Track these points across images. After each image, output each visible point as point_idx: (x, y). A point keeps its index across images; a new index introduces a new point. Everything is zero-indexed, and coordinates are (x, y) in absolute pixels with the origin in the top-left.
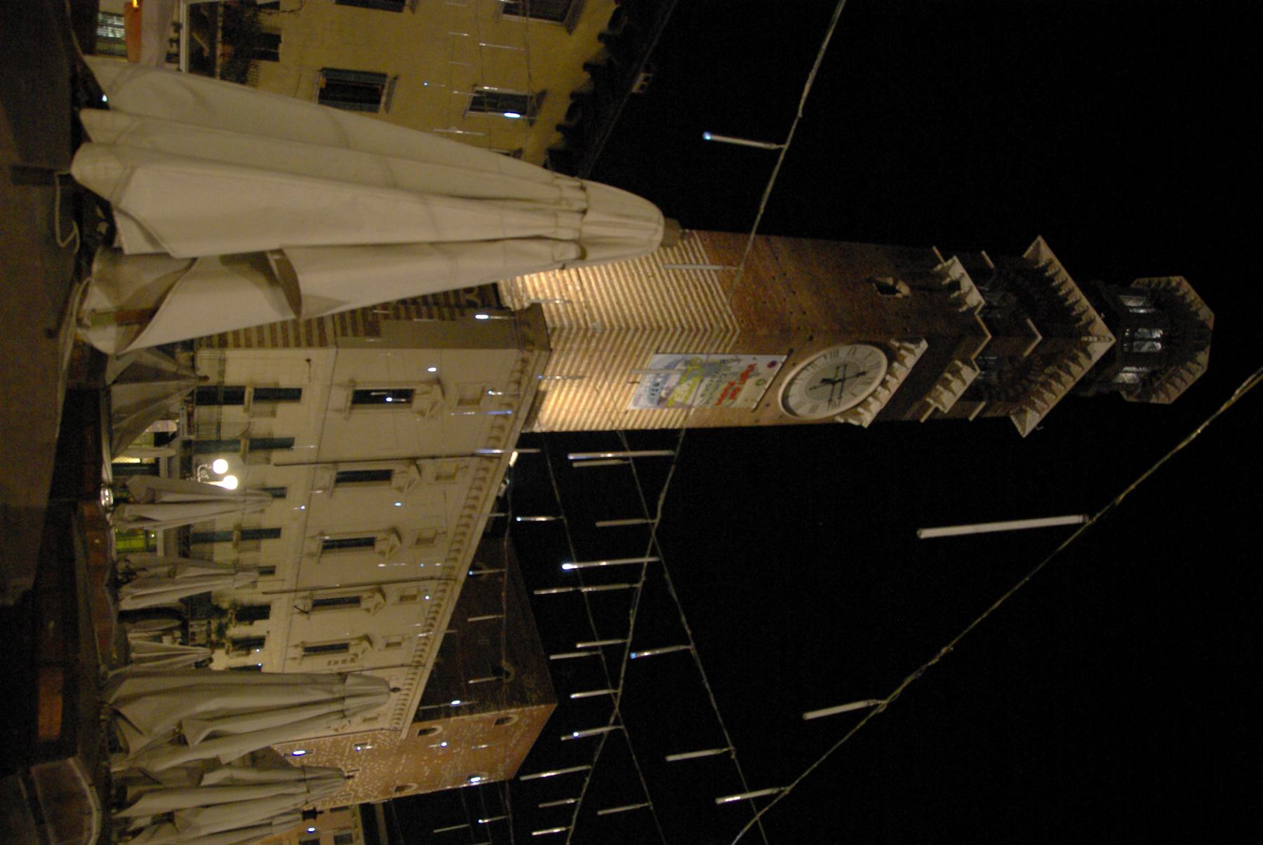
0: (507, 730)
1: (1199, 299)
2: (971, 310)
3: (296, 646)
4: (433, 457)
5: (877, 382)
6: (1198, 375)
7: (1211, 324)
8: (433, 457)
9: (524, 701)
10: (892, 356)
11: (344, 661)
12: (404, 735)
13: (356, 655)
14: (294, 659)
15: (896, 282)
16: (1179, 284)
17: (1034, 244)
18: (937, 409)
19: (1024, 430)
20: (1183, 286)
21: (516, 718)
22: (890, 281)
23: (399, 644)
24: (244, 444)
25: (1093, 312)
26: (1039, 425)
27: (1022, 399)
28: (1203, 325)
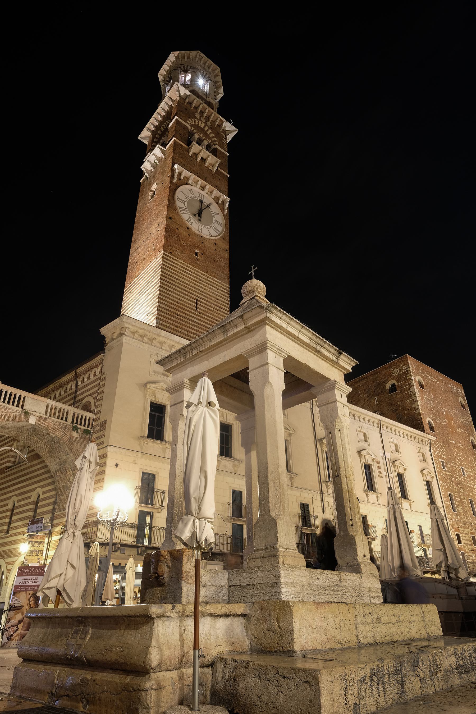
0: (427, 383)
1: (166, 62)
2: (163, 152)
6: (202, 55)
7: (177, 53)
9: (407, 373)
10: (186, 182)
11: (379, 468)
12: (434, 438)
13: (373, 459)
14: (377, 497)
15: (151, 191)
16: (162, 75)
17: (141, 140)
19: (234, 130)
20: (162, 73)
21: (418, 378)
22: (151, 193)
23: (365, 434)
25: (166, 99)
26: (230, 122)
28: (177, 58)
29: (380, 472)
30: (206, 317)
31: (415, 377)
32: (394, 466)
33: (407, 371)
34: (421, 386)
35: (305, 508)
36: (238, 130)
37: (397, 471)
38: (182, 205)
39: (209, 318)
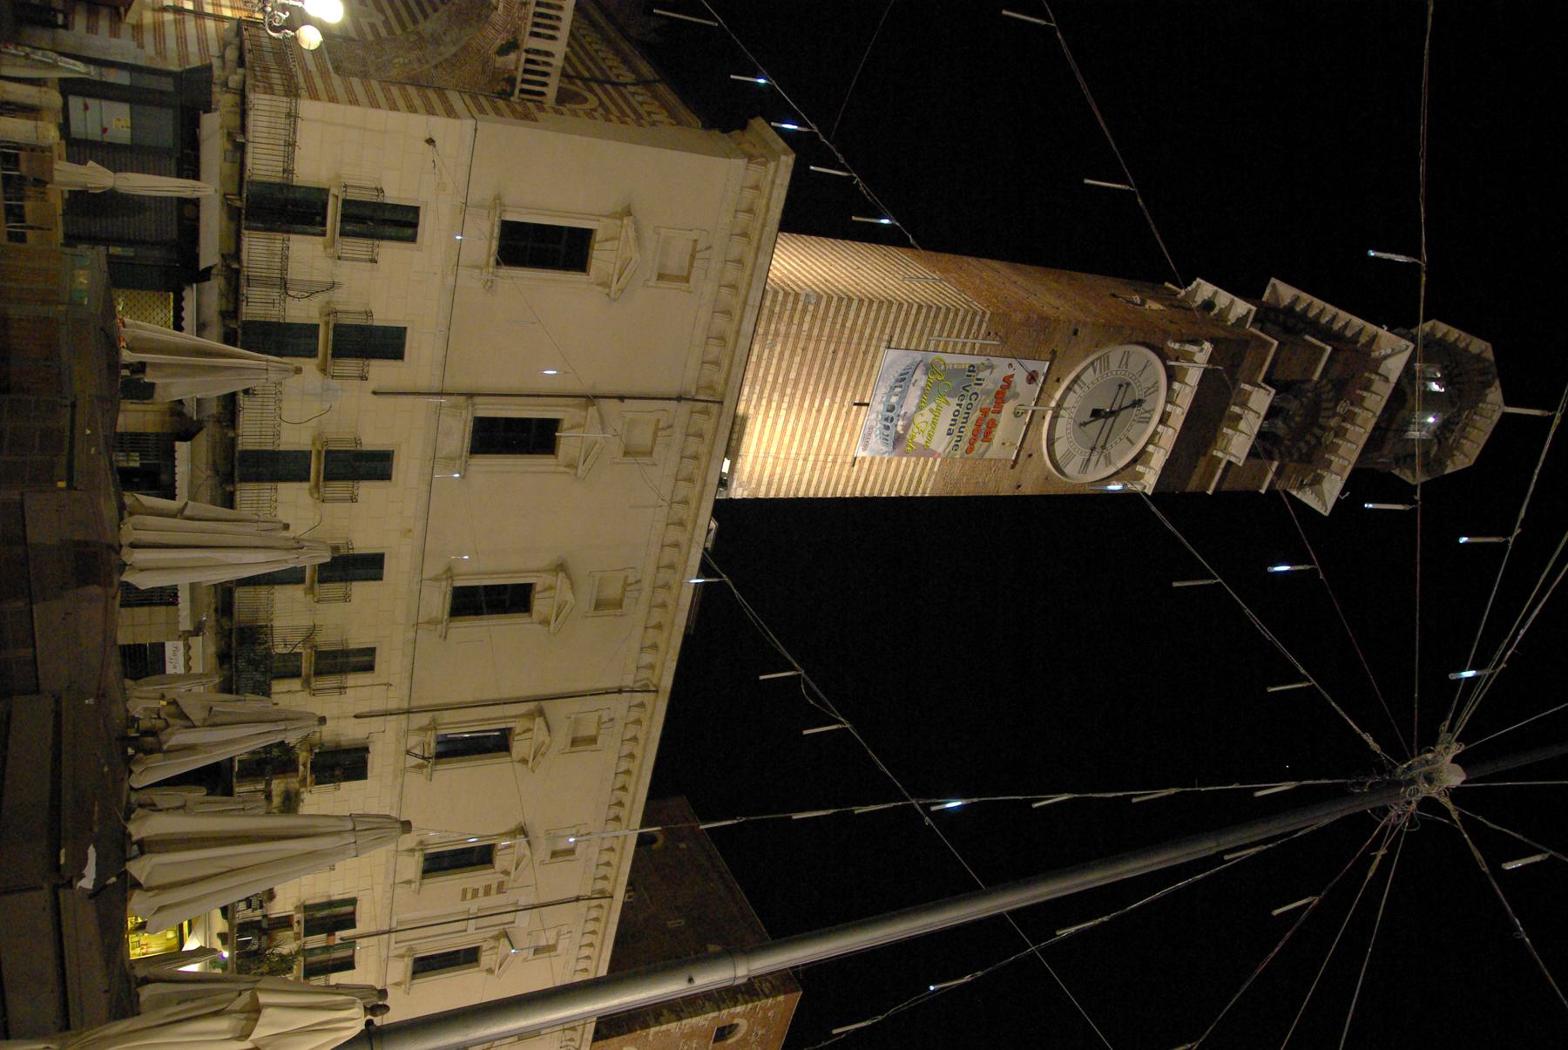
1: (1463, 334)
2: (1241, 321)
3: (402, 956)
4: (622, 398)
5: (1156, 418)
7: (1490, 355)
8: (622, 398)
13: (507, 873)
14: (409, 882)
16: (1433, 328)
18: (1229, 463)
19: (1324, 504)
21: (743, 1024)
24: (324, 339)
25: (1371, 328)
26: (1342, 493)
27: (1311, 460)
28: (1479, 358)
29: (475, 893)
30: (839, 431)
31: (743, 1016)
32: (496, 938)
33: (758, 995)
34: (723, 1033)
35: (362, 661)
36: (1326, 514)
37: (485, 946)
38: (1114, 365)
39: (837, 437)
